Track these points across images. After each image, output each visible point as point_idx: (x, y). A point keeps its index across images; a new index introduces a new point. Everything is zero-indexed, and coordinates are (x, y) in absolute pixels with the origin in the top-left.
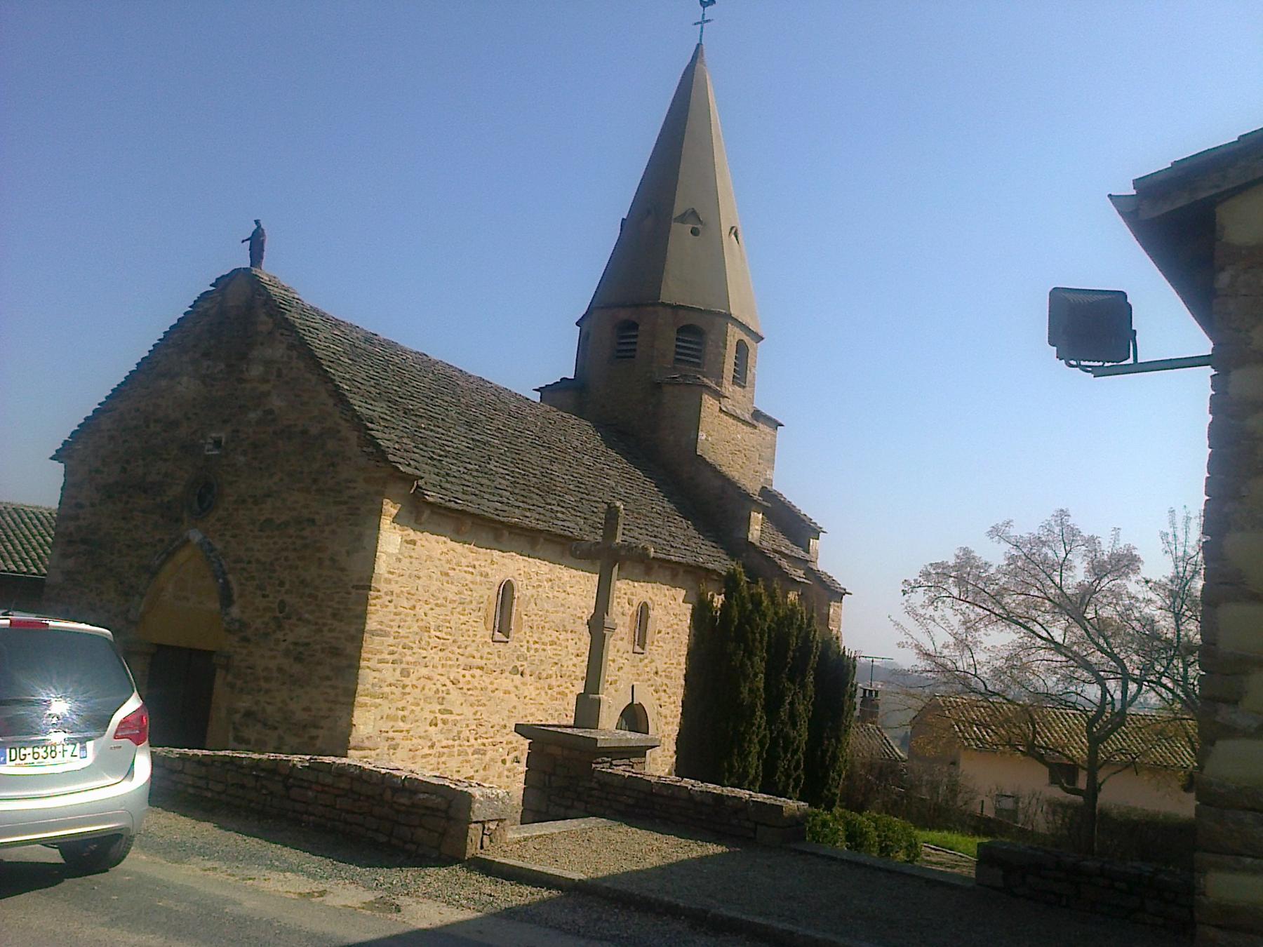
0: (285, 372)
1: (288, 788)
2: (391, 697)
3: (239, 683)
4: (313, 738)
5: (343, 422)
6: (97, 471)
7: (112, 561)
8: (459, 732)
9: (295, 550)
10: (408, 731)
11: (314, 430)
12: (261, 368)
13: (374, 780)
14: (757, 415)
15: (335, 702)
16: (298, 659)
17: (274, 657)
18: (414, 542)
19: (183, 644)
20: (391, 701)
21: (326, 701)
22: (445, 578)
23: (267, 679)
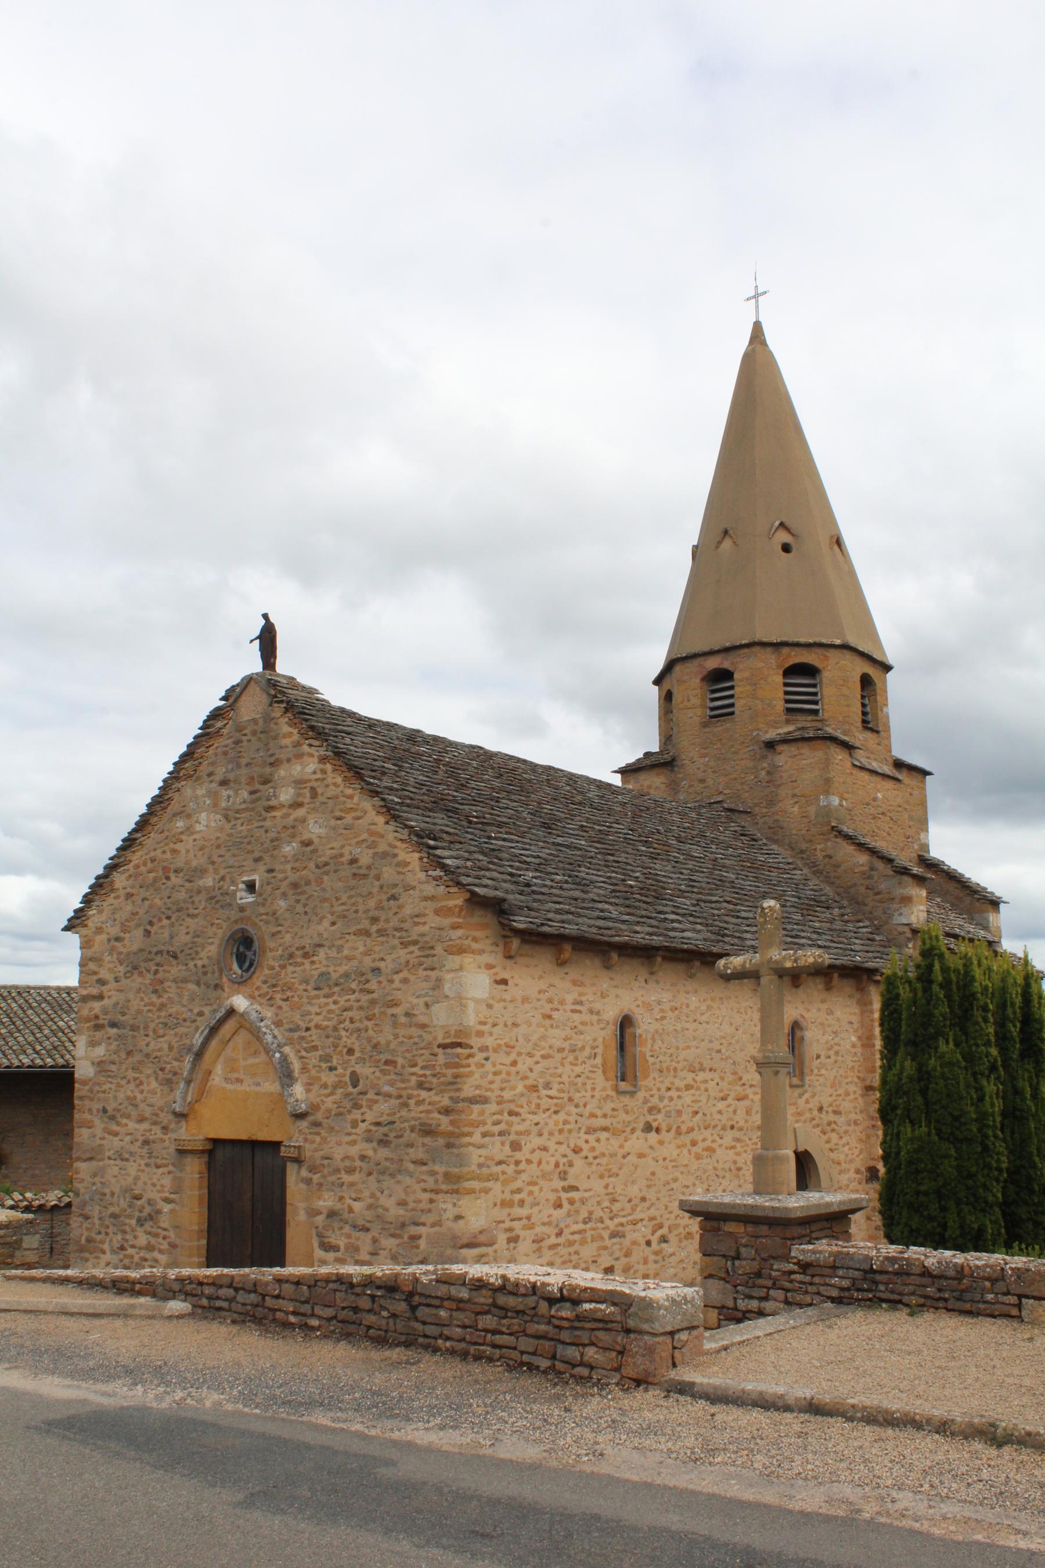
0: (320, 791)
1: (413, 1308)
2: (502, 1177)
3: (316, 1178)
5: (399, 844)
6: (117, 939)
7: (148, 1045)
8: (591, 1213)
9: (361, 1008)
10: (528, 1218)
11: (365, 860)
12: (291, 791)
13: (522, 1290)
14: (899, 764)
15: (437, 1192)
16: (383, 1142)
17: (353, 1143)
18: (504, 982)
19: (244, 1137)
20: (505, 1183)
21: (425, 1190)
22: (548, 1022)
23: (350, 1171)
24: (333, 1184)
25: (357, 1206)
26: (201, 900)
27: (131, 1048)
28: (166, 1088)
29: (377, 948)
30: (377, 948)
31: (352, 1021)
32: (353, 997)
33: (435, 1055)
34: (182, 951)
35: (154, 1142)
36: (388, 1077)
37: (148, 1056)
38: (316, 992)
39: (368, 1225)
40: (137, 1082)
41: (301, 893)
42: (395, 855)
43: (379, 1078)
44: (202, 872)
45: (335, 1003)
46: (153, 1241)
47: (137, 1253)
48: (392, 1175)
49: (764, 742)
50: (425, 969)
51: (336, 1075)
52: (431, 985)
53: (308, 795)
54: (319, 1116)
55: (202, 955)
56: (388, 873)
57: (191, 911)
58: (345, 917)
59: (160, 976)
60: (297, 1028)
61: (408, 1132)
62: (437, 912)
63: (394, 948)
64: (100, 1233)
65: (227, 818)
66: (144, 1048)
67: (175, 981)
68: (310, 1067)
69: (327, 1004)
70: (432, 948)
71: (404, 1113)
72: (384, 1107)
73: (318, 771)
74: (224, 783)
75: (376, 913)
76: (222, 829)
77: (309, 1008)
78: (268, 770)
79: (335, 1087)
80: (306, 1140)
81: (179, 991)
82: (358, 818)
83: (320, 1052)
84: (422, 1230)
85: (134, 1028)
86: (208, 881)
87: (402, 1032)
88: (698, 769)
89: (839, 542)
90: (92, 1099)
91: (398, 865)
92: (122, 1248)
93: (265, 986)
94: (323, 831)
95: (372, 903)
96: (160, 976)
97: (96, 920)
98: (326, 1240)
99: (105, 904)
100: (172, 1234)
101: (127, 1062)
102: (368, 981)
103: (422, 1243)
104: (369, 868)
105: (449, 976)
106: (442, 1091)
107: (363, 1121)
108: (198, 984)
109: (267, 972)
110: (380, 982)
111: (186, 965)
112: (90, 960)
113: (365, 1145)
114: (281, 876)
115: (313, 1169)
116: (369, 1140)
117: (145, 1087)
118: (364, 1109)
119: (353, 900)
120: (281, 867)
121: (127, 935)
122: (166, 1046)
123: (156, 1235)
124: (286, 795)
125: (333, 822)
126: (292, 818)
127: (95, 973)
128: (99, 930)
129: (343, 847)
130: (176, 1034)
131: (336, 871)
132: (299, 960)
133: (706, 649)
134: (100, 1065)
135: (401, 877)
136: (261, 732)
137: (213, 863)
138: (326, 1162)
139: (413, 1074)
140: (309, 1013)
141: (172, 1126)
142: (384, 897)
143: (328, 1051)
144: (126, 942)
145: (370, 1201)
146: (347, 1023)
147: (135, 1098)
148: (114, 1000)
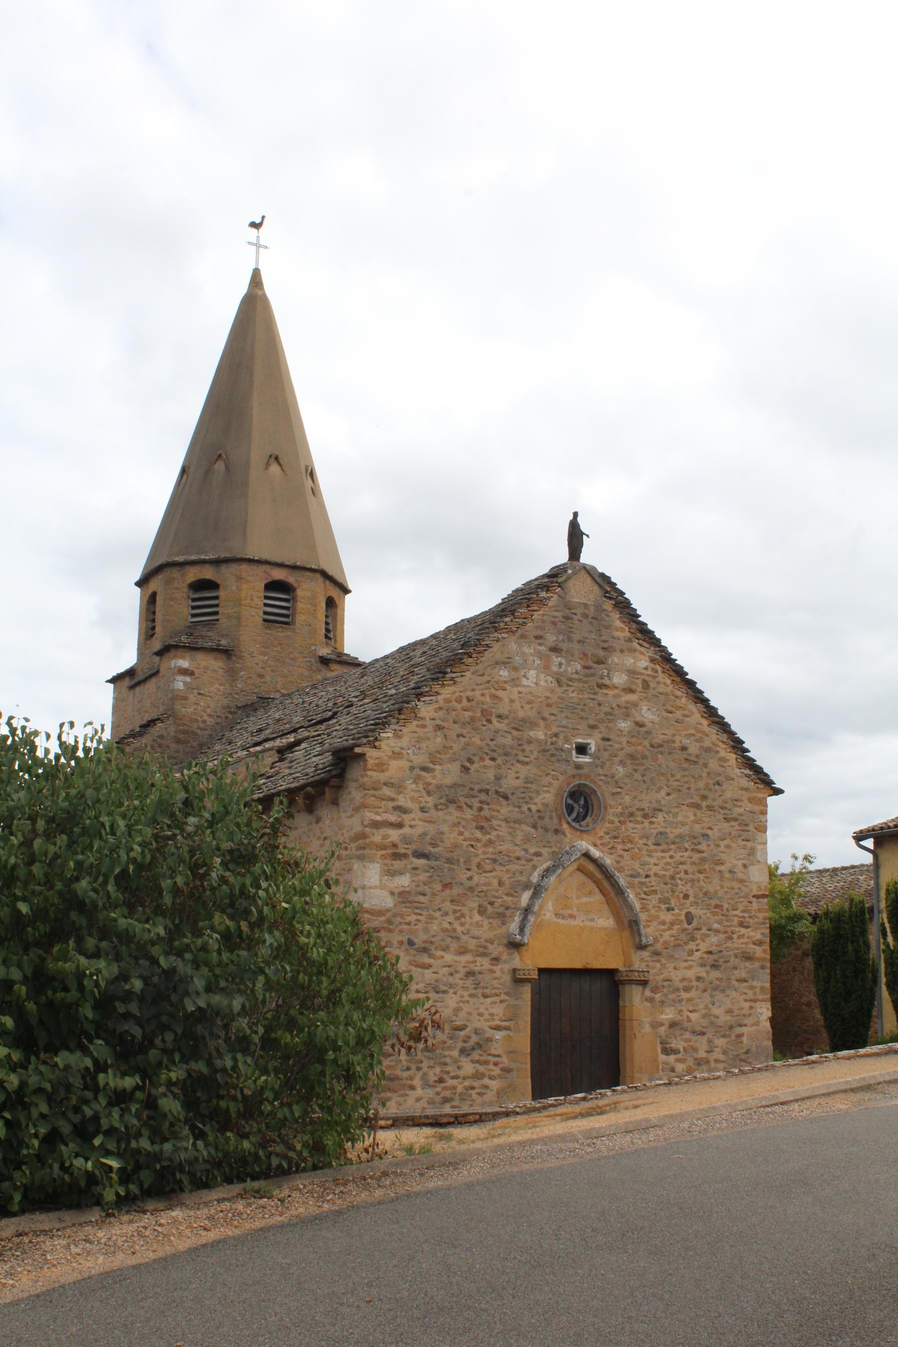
0: (652, 685)
3: (658, 997)
4: (739, 1036)
5: (720, 744)
6: (424, 769)
7: (470, 878)
9: (694, 863)
11: (693, 749)
12: (625, 677)
15: (755, 1001)
16: (715, 966)
17: (689, 968)
19: (578, 965)
21: (746, 1000)
23: (687, 989)
24: (674, 1001)
25: (693, 1016)
26: (532, 752)
27: (448, 880)
28: (496, 922)
29: (706, 819)
30: (706, 819)
31: (686, 872)
32: (686, 854)
33: (750, 902)
34: (513, 794)
35: (480, 973)
36: (717, 918)
37: (471, 889)
38: (655, 847)
39: (704, 1030)
40: (458, 914)
41: (638, 764)
42: (717, 752)
43: (709, 918)
44: (534, 725)
45: (671, 857)
46: (481, 1069)
47: (460, 1083)
48: (723, 991)
49: (321, 657)
50: (743, 840)
51: (673, 915)
52: (747, 852)
53: (640, 686)
54: (658, 947)
55: (537, 800)
56: (713, 765)
57: (521, 758)
58: (679, 791)
59: (486, 813)
60: (638, 875)
61: (733, 958)
62: (750, 800)
63: (719, 820)
64: (408, 1069)
65: (558, 682)
66: (465, 881)
67: (506, 820)
68: (650, 907)
69: (664, 857)
70: (746, 825)
71: (729, 944)
72: (714, 939)
73: (650, 669)
74: (555, 650)
75: (706, 793)
76: (553, 691)
77: (647, 859)
78: (601, 653)
79: (672, 924)
80: (647, 966)
81: (510, 830)
82: (686, 716)
83: (659, 896)
84: (745, 1030)
85: (449, 861)
86: (539, 734)
87: (726, 884)
88: (257, 664)
89: (184, 471)
90: (391, 931)
91: (721, 759)
92: (441, 1080)
93: (607, 837)
94: (655, 718)
95: (701, 784)
96: (486, 813)
97: (392, 744)
98: (668, 1046)
99: (405, 730)
100: (505, 1060)
101: (444, 894)
102: (699, 843)
103: (744, 1039)
104: (697, 756)
105: (759, 847)
106: (756, 929)
107: (697, 951)
108: (534, 826)
109: (607, 825)
110: (709, 845)
111: (520, 807)
112: (385, 784)
113: (700, 969)
114: (617, 746)
115: (655, 990)
116: (702, 965)
117: (468, 919)
118: (699, 941)
119: (686, 779)
120: (618, 739)
121: (437, 767)
122: (495, 882)
123: (486, 1063)
124: (619, 679)
125: (664, 714)
126: (623, 699)
127: (393, 800)
128: (396, 755)
129: (674, 735)
130: (507, 871)
131: (670, 753)
132: (639, 819)
133: (279, 561)
134: (403, 896)
135: (722, 769)
136: (593, 618)
137: (544, 719)
138: (666, 984)
139: (734, 916)
140: (648, 864)
141: (504, 957)
142: (711, 782)
143: (666, 895)
144: (436, 773)
145: (704, 1011)
146: (682, 873)
147: (455, 930)
148: (420, 830)
